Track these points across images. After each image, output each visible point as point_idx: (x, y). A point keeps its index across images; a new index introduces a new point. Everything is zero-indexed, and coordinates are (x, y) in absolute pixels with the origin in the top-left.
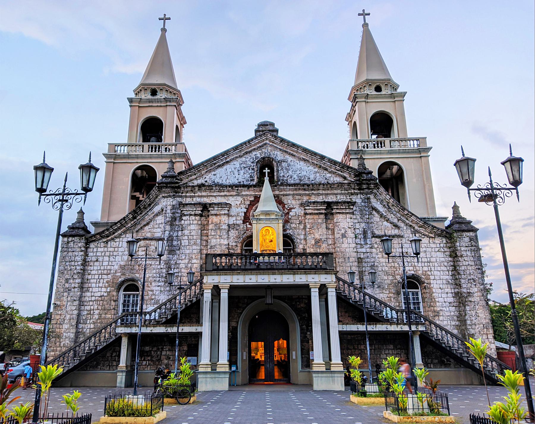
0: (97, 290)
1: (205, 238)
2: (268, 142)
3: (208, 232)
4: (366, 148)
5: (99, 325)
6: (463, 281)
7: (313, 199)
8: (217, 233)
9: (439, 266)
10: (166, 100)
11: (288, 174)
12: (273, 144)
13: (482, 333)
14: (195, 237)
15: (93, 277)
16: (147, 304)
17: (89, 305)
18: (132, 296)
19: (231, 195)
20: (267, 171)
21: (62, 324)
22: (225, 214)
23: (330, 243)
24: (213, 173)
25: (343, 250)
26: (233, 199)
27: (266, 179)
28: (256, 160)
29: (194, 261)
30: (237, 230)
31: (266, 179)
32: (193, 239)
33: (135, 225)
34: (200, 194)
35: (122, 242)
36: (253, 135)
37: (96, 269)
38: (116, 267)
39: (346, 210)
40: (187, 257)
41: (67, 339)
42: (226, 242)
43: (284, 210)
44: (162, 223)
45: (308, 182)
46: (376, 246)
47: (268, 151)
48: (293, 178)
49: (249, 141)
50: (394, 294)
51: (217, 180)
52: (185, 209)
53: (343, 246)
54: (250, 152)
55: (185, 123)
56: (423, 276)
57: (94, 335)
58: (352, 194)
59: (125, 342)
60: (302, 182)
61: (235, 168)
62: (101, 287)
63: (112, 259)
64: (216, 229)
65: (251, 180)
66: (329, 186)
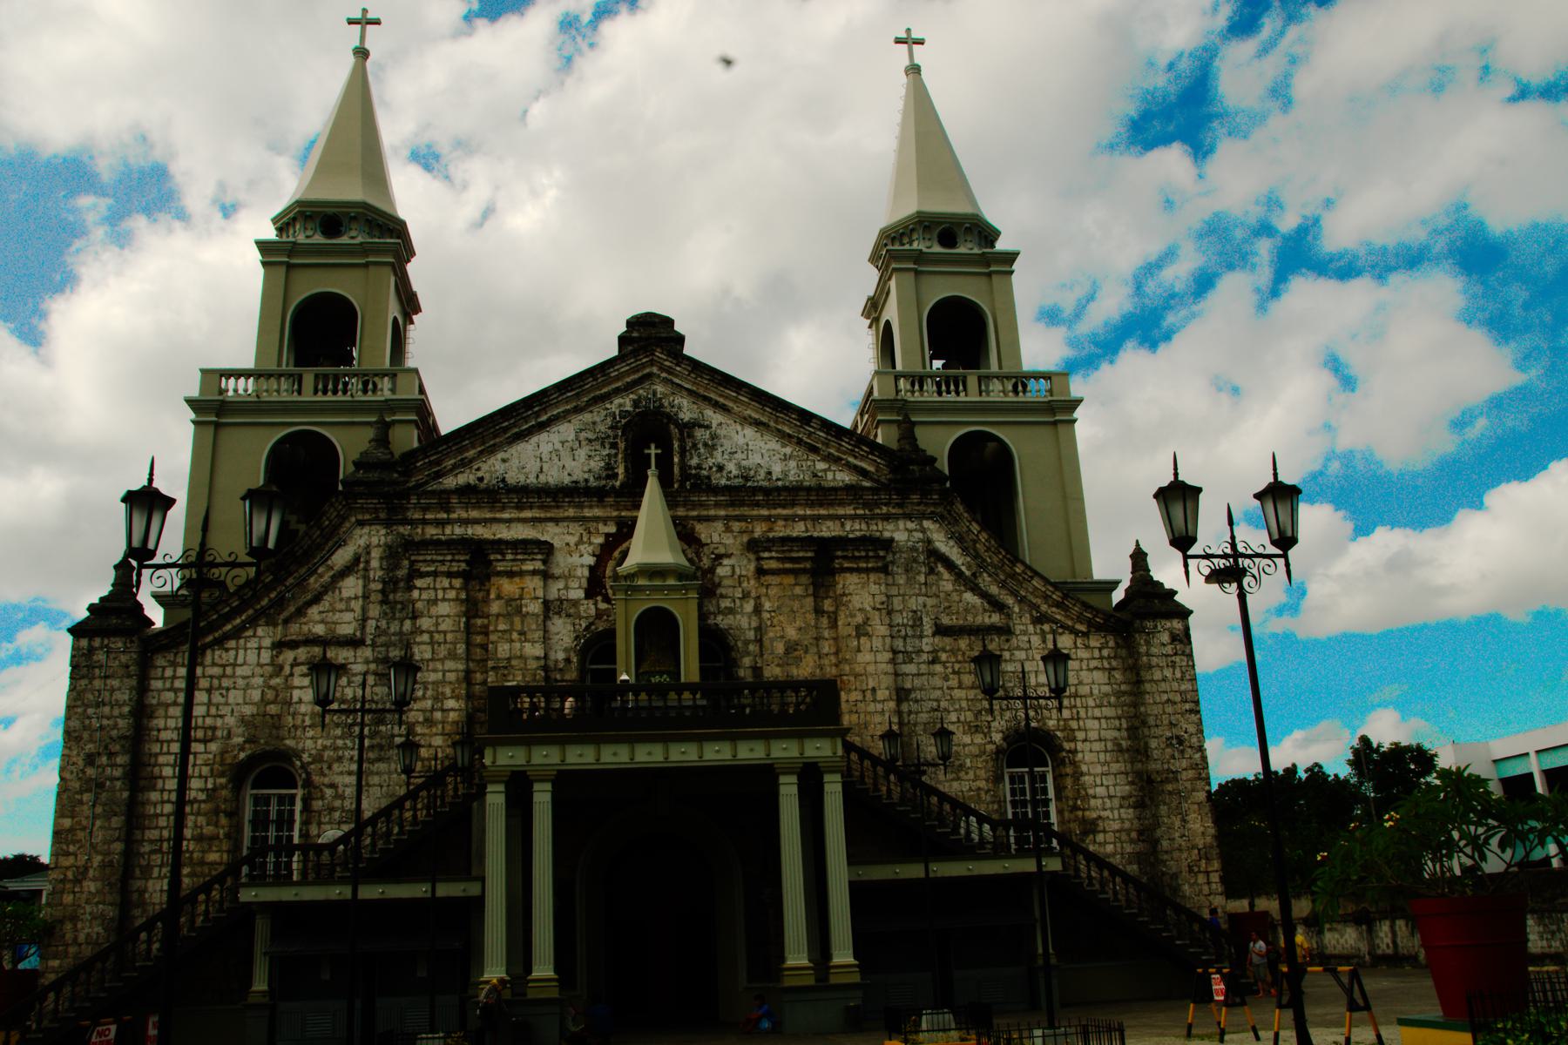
1: (479, 639)
2: (655, 370)
3: (486, 621)
6: (1153, 744)
7: (780, 530)
8: (512, 624)
9: (1097, 706)
10: (364, 250)
11: (711, 461)
12: (670, 377)
13: (1196, 869)
14: (449, 637)
15: (165, 749)
16: (320, 824)
17: (156, 827)
18: (274, 802)
20: (653, 451)
21: (80, 882)
22: (534, 573)
25: (859, 669)
26: (557, 530)
27: (652, 473)
28: (623, 421)
30: (569, 616)
31: (652, 473)
32: (445, 642)
33: (280, 603)
34: (464, 515)
35: (246, 649)
36: (614, 352)
37: (173, 725)
38: (231, 721)
39: (867, 562)
40: (429, 693)
41: (95, 923)
42: (538, 651)
43: (700, 560)
44: (356, 598)
45: (765, 484)
46: (944, 657)
48: (724, 474)
50: (987, 780)
51: (513, 477)
52: (421, 558)
54: (606, 397)
55: (417, 310)
56: (1059, 733)
59: (262, 927)
60: (749, 484)
61: (563, 443)
63: (217, 698)
65: (608, 477)
66: (821, 495)
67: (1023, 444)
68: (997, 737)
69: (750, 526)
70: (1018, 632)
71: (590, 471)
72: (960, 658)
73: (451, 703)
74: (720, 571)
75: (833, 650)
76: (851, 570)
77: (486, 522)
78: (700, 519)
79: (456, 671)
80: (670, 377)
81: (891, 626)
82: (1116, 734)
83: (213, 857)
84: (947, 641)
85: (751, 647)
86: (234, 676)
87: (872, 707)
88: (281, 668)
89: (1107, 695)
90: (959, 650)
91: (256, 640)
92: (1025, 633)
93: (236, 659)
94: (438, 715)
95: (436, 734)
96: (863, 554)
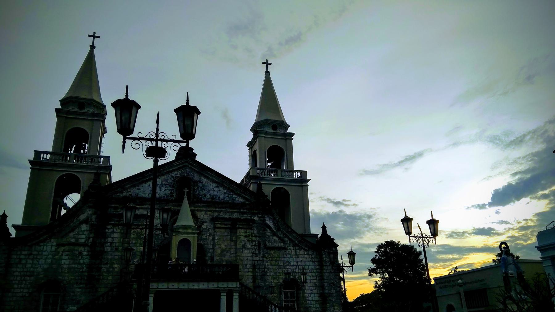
0: (18, 290)
4: (263, 175)
7: (222, 215)
9: (310, 272)
15: (15, 279)
23: (233, 252)
24: (137, 188)
25: (242, 258)
29: (116, 266)
35: (47, 246)
38: (40, 270)
46: (267, 255)
47: (187, 172)
53: (243, 255)
54: (172, 171)
56: (299, 280)
60: (213, 201)
62: (23, 288)
63: (35, 262)
66: (233, 206)
67: (292, 191)
68: (281, 281)
69: (213, 213)
70: (288, 249)
71: (165, 194)
72: (271, 256)
73: (116, 266)
74: (203, 227)
75: (235, 252)
76: (241, 228)
78: (198, 211)
79: (118, 255)
81: (252, 245)
82: (315, 281)
85: (211, 251)
86: (42, 254)
87: (246, 270)
88: (59, 253)
89: (313, 269)
90: (271, 253)
91: (51, 243)
92: (290, 249)
93: (43, 249)
95: (110, 276)
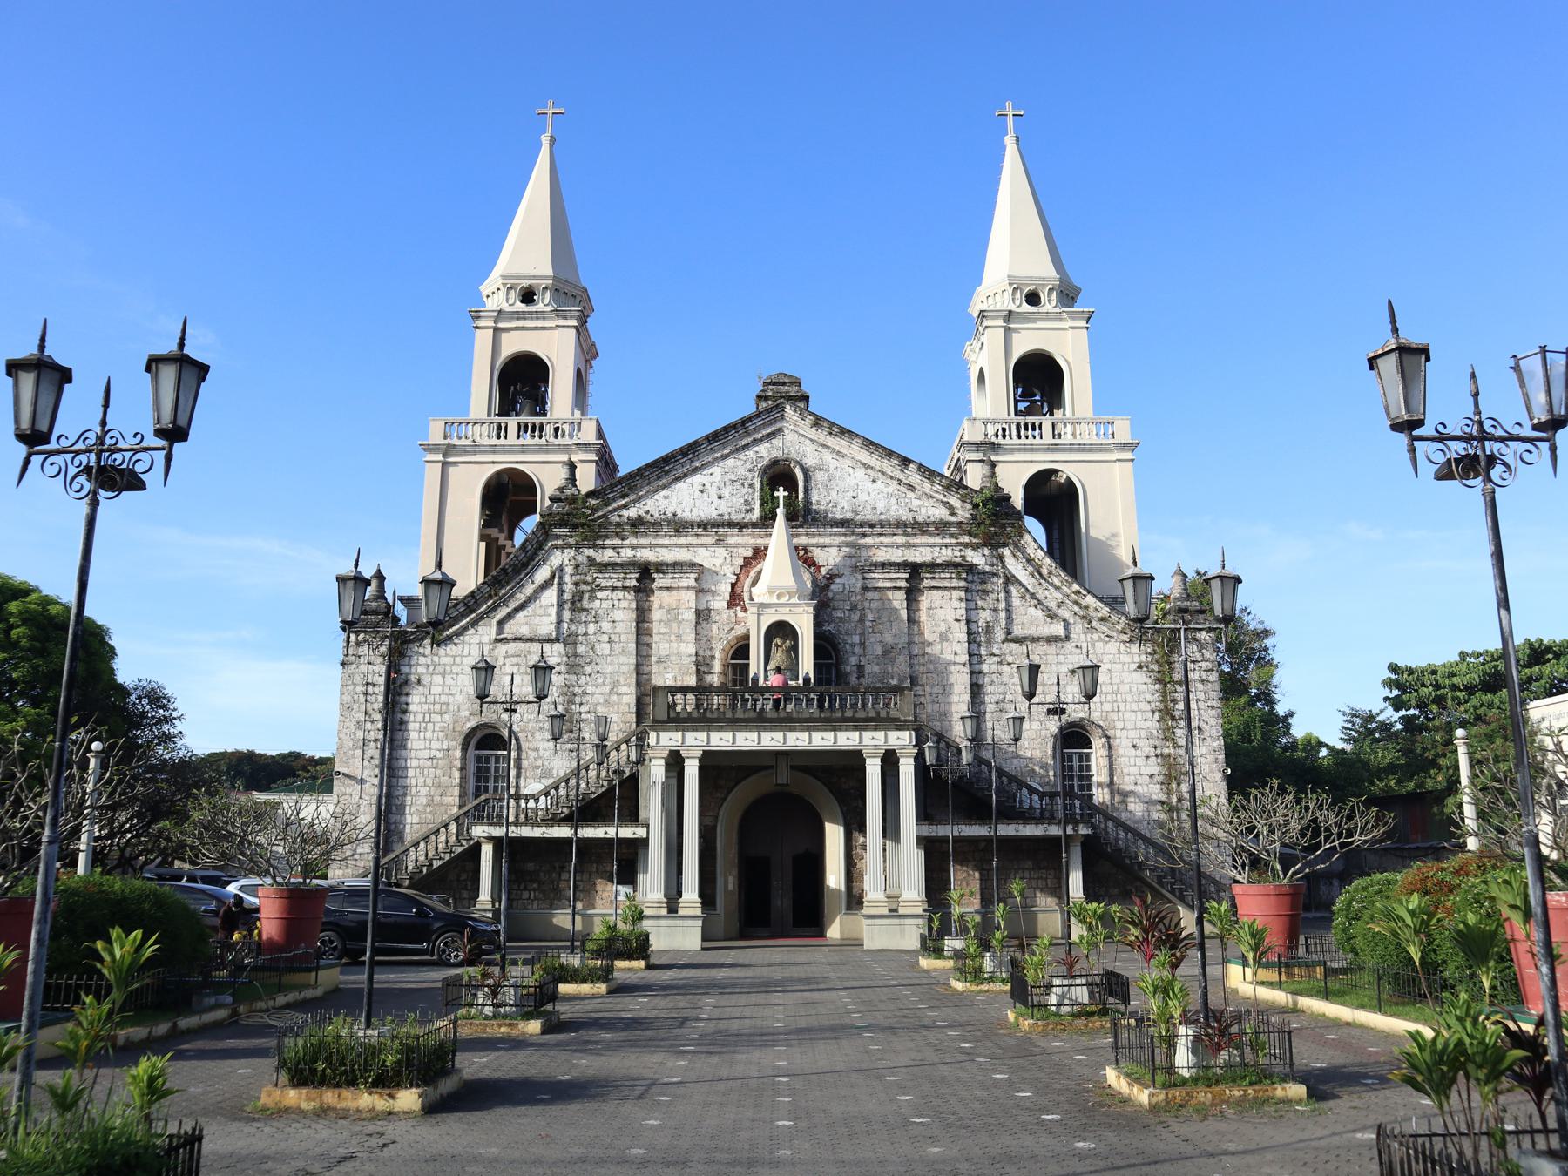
0: (421, 745)
4: (1000, 437)
5: (430, 817)
8: (671, 628)
14: (623, 638)
16: (526, 778)
18: (493, 759)
19: (702, 545)
20: (781, 493)
22: (688, 588)
28: (759, 466)
32: (620, 642)
38: (459, 698)
40: (608, 681)
48: (839, 507)
49: (744, 422)
57: (426, 838)
58: (966, 545)
59: (487, 851)
60: (858, 517)
62: (431, 740)
63: (449, 680)
64: (669, 621)
65: (748, 511)
66: (919, 527)
77: (651, 546)
80: (797, 429)
83: (447, 800)
84: (1014, 646)
85: (857, 649)
94: (615, 698)
96: (948, 575)
